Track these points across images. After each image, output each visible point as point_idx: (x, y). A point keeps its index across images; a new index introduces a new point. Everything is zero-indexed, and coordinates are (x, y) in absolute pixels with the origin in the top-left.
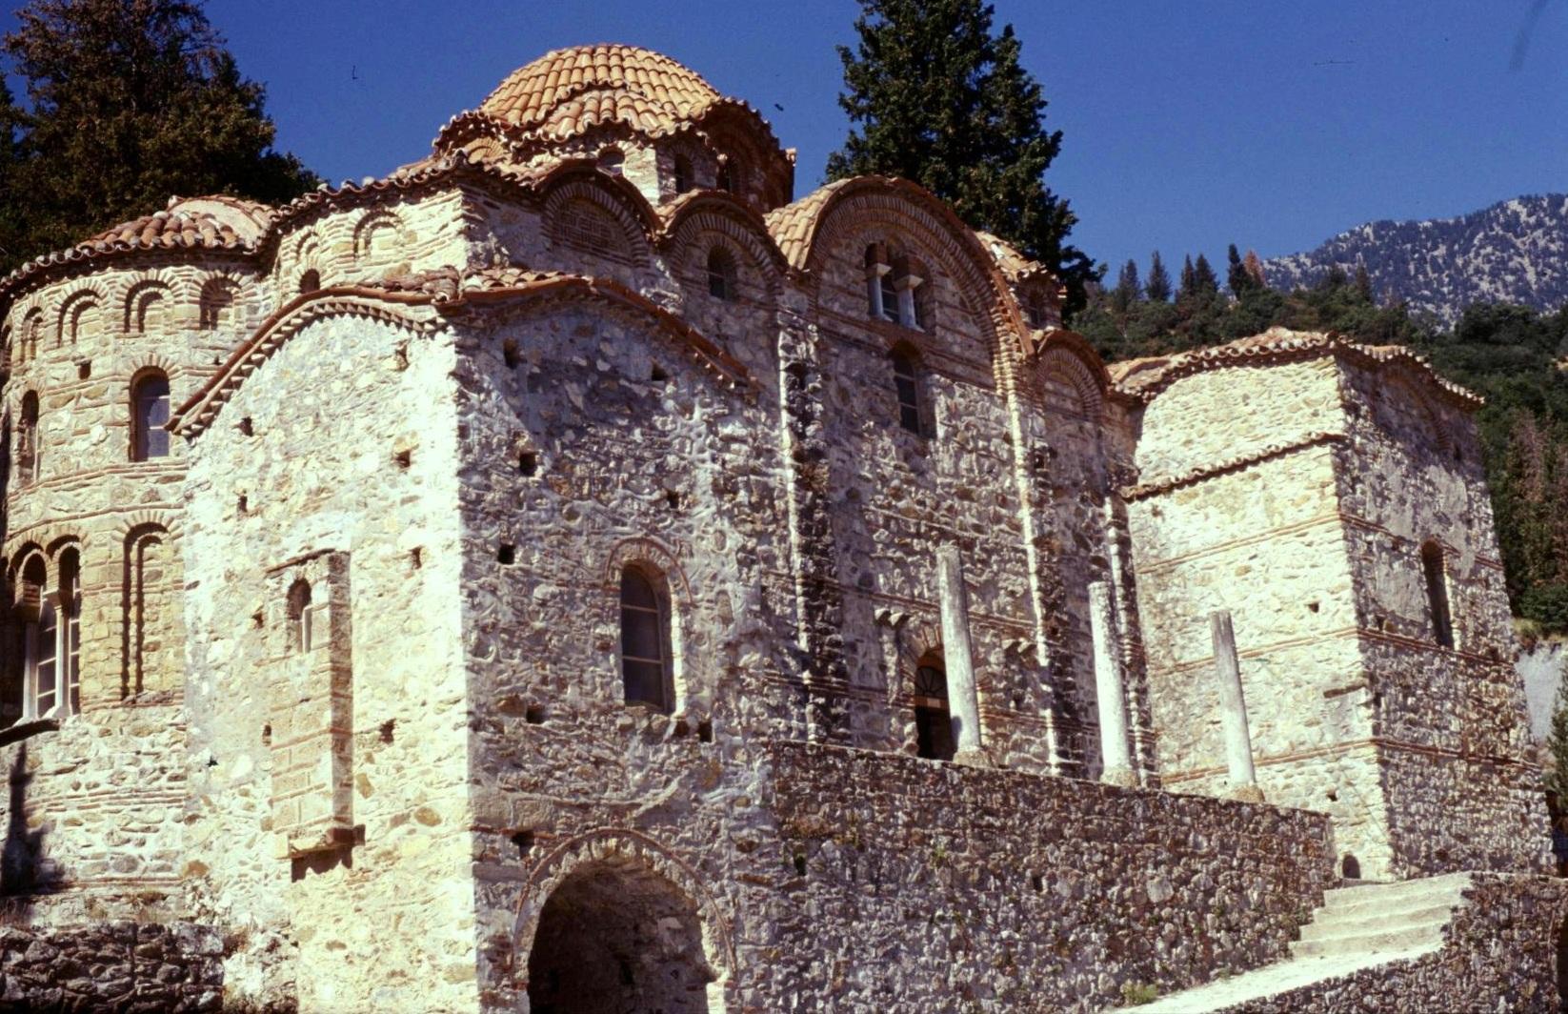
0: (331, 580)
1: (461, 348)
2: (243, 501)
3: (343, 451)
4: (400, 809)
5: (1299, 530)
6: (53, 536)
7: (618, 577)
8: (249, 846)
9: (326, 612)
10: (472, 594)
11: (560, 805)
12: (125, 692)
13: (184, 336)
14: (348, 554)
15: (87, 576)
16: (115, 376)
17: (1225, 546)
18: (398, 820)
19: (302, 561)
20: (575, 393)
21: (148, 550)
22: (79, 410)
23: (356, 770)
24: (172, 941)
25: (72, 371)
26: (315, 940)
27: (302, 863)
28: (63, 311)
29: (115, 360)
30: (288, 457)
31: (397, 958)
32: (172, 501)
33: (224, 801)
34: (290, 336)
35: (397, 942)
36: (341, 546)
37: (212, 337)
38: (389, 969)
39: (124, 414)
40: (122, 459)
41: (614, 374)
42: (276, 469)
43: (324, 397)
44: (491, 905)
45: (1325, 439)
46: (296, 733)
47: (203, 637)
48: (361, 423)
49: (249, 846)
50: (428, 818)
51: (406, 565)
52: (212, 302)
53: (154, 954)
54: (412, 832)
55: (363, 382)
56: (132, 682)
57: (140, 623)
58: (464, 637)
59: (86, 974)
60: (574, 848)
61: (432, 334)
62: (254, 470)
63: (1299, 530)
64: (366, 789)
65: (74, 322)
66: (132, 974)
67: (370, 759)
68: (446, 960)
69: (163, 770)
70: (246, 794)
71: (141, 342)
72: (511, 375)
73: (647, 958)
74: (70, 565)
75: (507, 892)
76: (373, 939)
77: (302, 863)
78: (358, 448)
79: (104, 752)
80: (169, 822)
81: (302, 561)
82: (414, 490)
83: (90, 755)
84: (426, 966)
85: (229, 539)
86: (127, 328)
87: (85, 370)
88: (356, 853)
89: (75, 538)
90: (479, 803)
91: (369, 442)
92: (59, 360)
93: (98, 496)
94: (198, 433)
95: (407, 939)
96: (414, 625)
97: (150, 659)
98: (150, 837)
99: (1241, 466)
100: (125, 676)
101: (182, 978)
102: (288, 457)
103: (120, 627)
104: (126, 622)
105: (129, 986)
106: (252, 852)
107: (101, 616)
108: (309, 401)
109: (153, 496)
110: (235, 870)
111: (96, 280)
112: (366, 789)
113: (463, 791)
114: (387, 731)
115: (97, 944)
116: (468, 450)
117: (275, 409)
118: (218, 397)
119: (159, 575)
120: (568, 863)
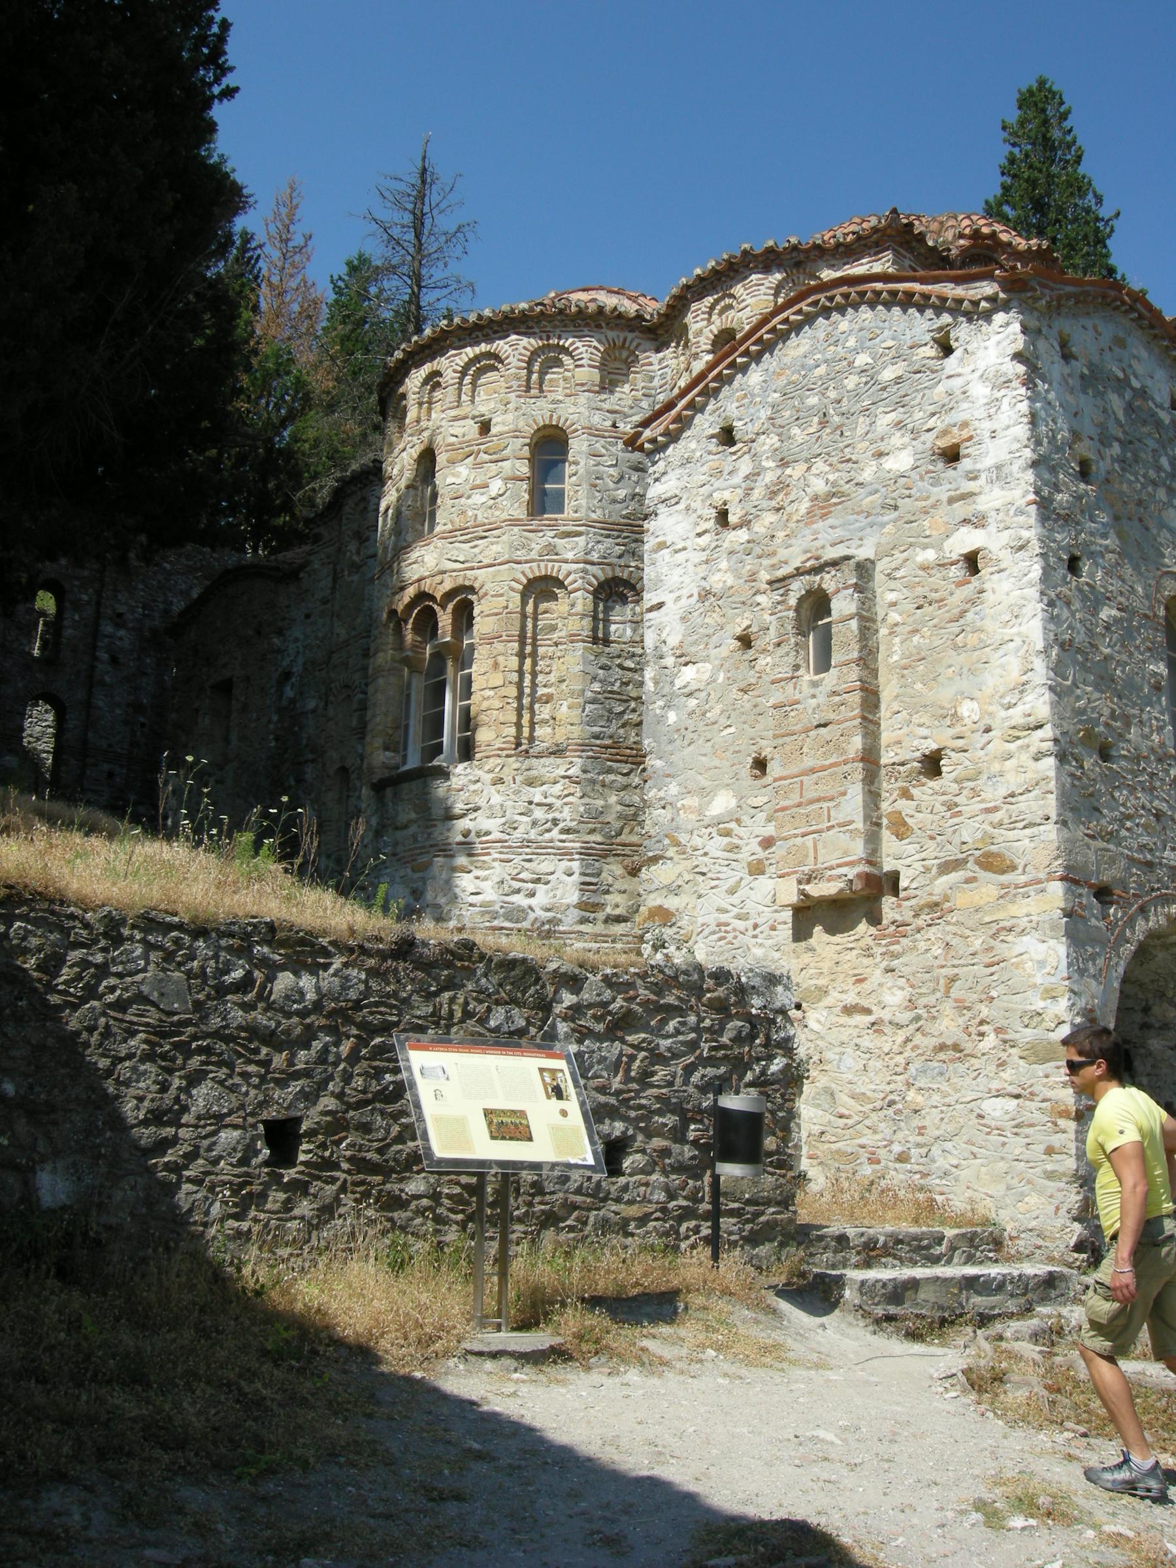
0: (858, 588)
1: (1025, 330)
2: (722, 517)
3: (862, 449)
4: (952, 852)
6: (448, 585)
7: (1162, 612)
8: (732, 891)
9: (854, 624)
10: (1051, 604)
11: (1132, 860)
12: (518, 744)
13: (583, 398)
14: (873, 562)
15: (482, 625)
16: (516, 433)
18: (947, 867)
19: (816, 570)
20: (1116, 403)
21: (543, 606)
22: (478, 465)
23: (885, 806)
24: (742, 991)
25: (470, 429)
26: (828, 1001)
27: (811, 915)
28: (464, 373)
30: (784, 463)
31: (948, 1026)
32: (570, 556)
33: (697, 841)
34: (783, 336)
35: (948, 1008)
36: (864, 552)
37: (611, 401)
38: (933, 1042)
39: (524, 469)
40: (521, 513)
41: (1143, 393)
42: (769, 477)
43: (832, 394)
44: (1082, 972)
46: (809, 762)
47: (669, 661)
48: (885, 421)
49: (732, 891)
50: (994, 863)
51: (958, 572)
52: (613, 372)
53: (721, 1007)
54: (968, 881)
55: (888, 374)
56: (526, 732)
57: (534, 674)
58: (1046, 651)
59: (646, 1028)
60: (1143, 910)
61: (987, 316)
62: (737, 479)
64: (901, 829)
65: (474, 384)
66: (696, 1029)
67: (906, 794)
68: (1027, 1035)
69: (555, 822)
70: (728, 833)
71: (541, 403)
72: (1067, 370)
73: (1155, 1044)
74: (464, 615)
75: (1093, 957)
76: (911, 1004)
77: (811, 915)
78: (883, 447)
79: (496, 799)
80: (559, 874)
81: (816, 570)
82: (972, 486)
83: (482, 802)
84: (991, 1040)
85: (703, 556)
86: (528, 388)
87: (485, 427)
88: (888, 902)
89: (471, 589)
90: (1068, 848)
91: (897, 439)
92: (456, 419)
93: (493, 549)
94: (665, 447)
95: (962, 1007)
96: (972, 639)
97: (543, 712)
98: (541, 889)
100: (519, 726)
101: (752, 1037)
102: (784, 463)
103: (515, 677)
104: (521, 672)
105: (693, 1045)
106: (735, 899)
107: (496, 665)
108: (813, 400)
109: (551, 550)
110: (712, 919)
111: (500, 346)
112: (901, 829)
113: (1050, 833)
114: (932, 764)
115: (658, 989)
116: (1038, 443)
117: (764, 414)
118: (691, 405)
119: (553, 628)
120: (1141, 927)
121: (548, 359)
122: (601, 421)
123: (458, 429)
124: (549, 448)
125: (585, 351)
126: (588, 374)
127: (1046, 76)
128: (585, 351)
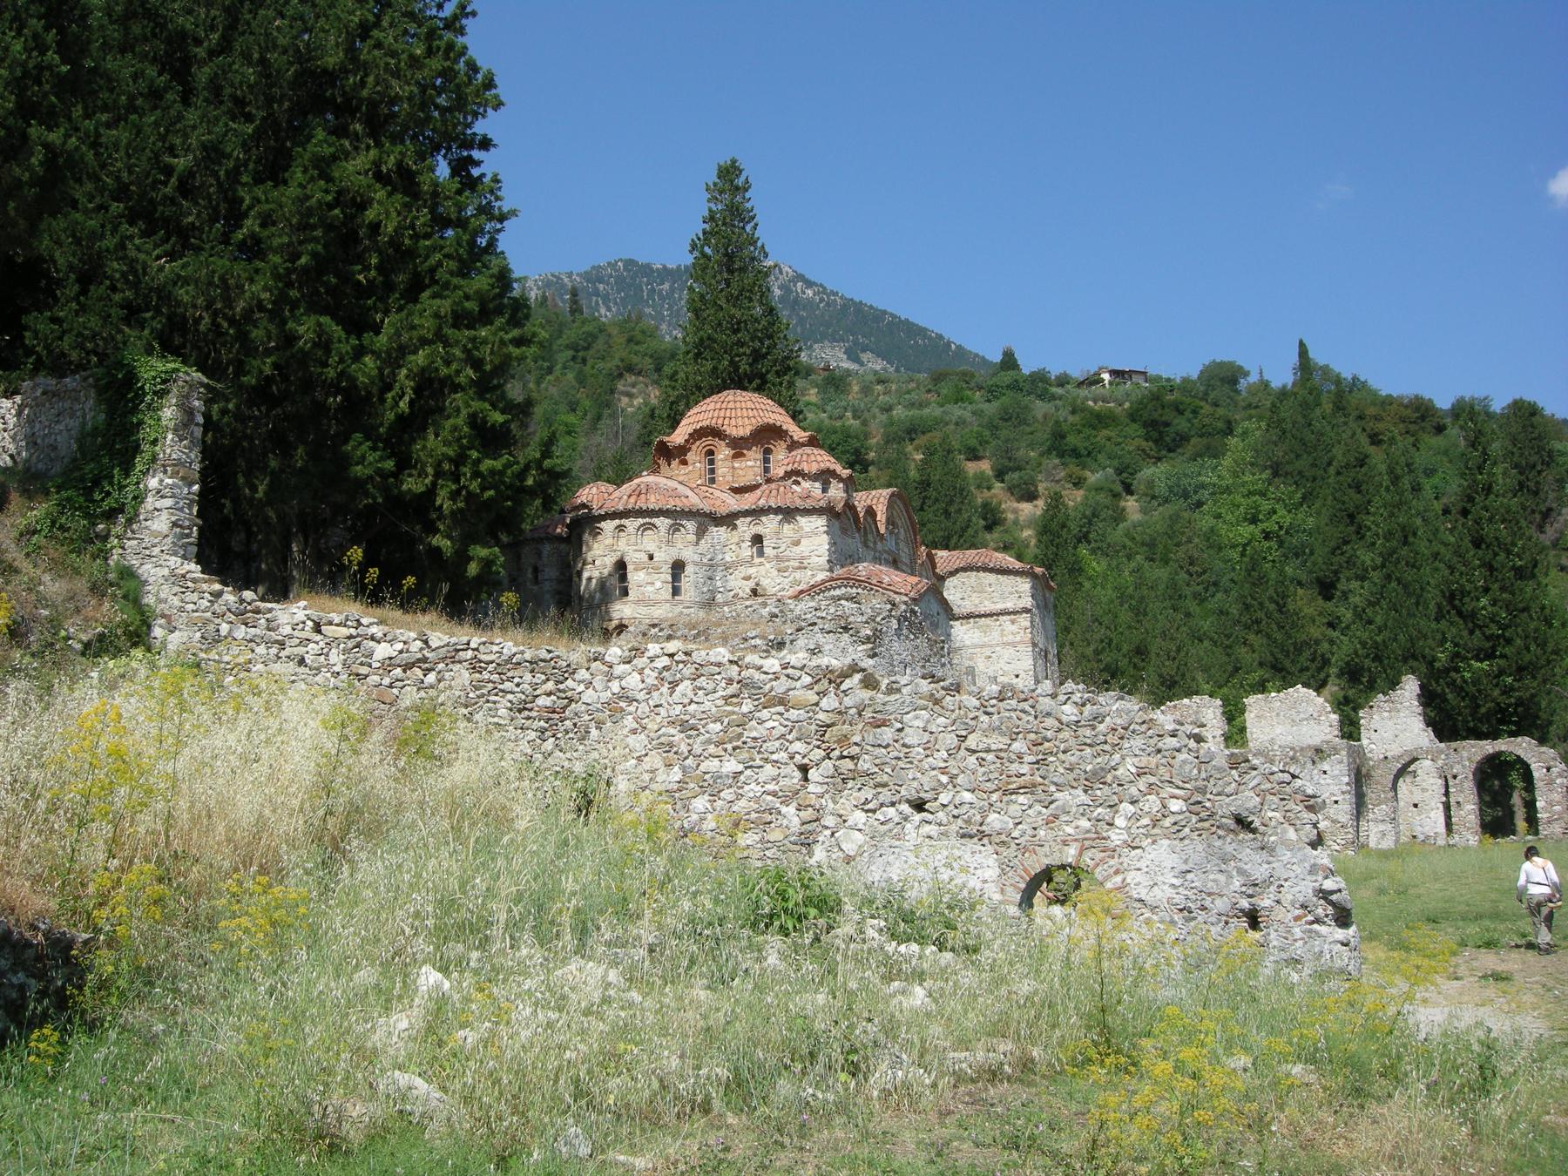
5: (1014, 645)
16: (666, 562)
17: (982, 646)
25: (646, 558)
29: (664, 557)
40: (669, 597)
45: (1027, 611)
52: (701, 533)
63: (1014, 645)
87: (651, 557)
99: (991, 615)
121: (675, 528)
122: (697, 558)
123: (637, 555)
124: (678, 567)
125: (691, 525)
126: (692, 538)
127: (742, 163)
128: (691, 525)
